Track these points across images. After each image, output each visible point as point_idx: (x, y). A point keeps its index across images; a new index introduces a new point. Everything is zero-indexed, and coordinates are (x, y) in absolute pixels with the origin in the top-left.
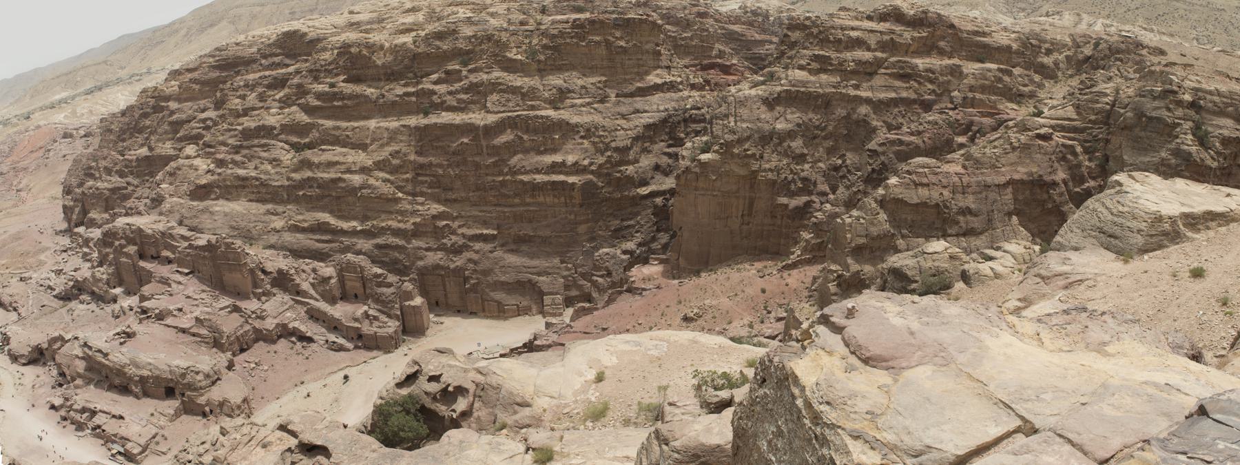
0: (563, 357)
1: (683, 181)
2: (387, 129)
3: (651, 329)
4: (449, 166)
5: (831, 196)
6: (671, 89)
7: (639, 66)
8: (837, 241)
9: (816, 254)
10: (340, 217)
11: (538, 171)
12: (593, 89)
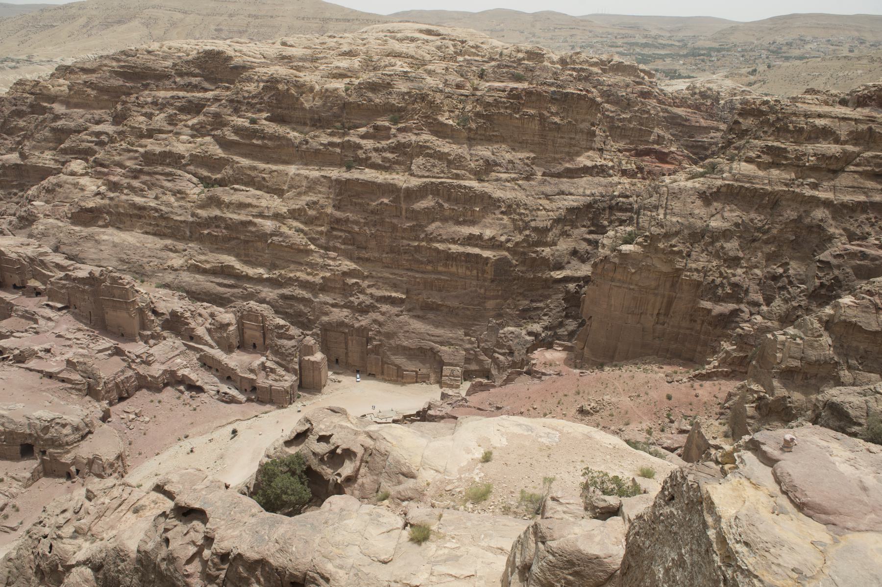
0: (453, 430)
1: (599, 271)
2: (307, 177)
3: (545, 415)
4: (366, 224)
5: (764, 308)
6: (602, 172)
7: (571, 145)
8: (763, 358)
9: (736, 368)
11: (454, 241)
12: (520, 165)
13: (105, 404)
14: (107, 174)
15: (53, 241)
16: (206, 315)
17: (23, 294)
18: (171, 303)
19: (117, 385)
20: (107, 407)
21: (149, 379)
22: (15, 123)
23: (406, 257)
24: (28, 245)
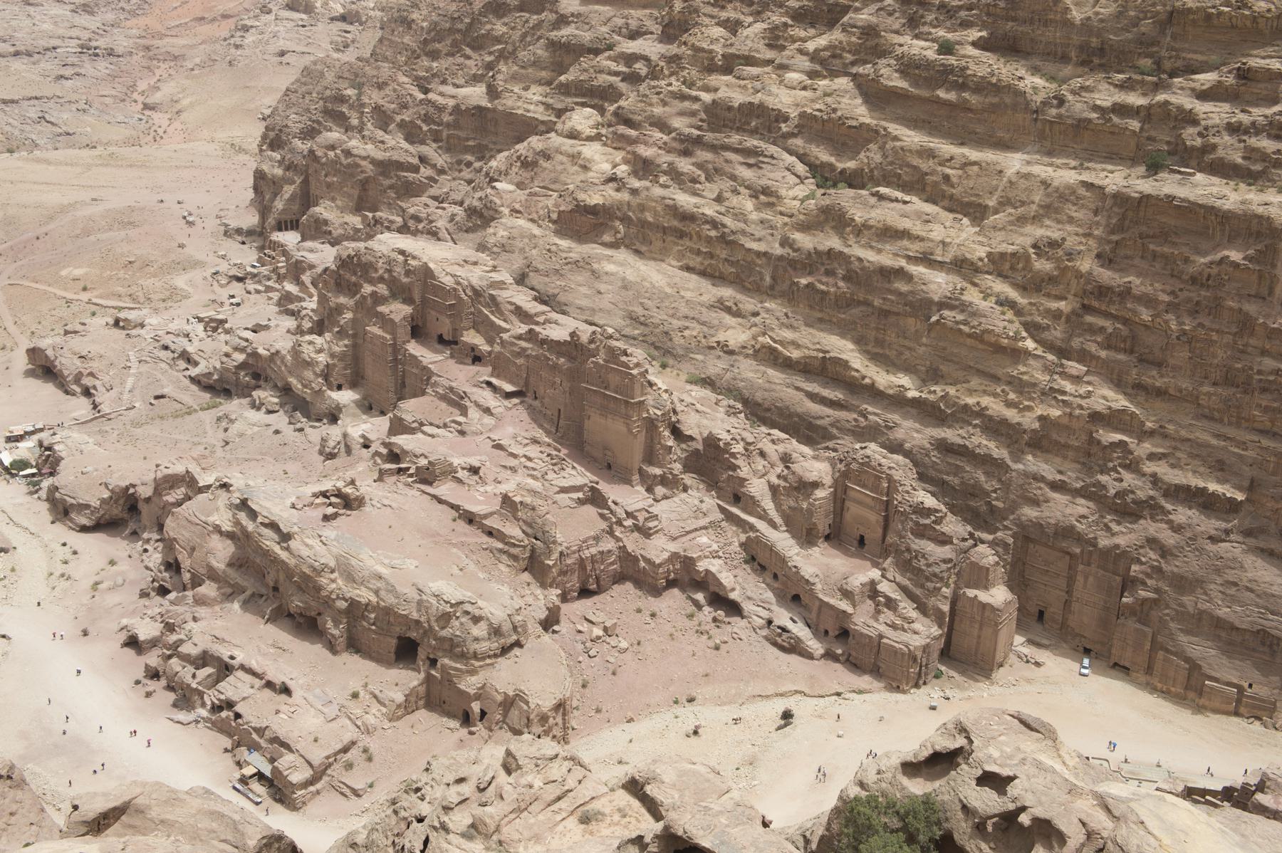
2: (1045, 184)
4: (1171, 307)
10: (876, 358)
13: (554, 594)
14: (634, 142)
15: (518, 263)
16: (774, 457)
17: (452, 356)
18: (709, 418)
19: (581, 562)
20: (558, 603)
21: (642, 564)
22: (488, 27)
23: (1265, 400)
24: (475, 263)
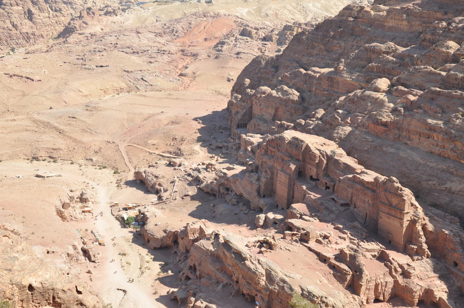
24: (329, 145)
